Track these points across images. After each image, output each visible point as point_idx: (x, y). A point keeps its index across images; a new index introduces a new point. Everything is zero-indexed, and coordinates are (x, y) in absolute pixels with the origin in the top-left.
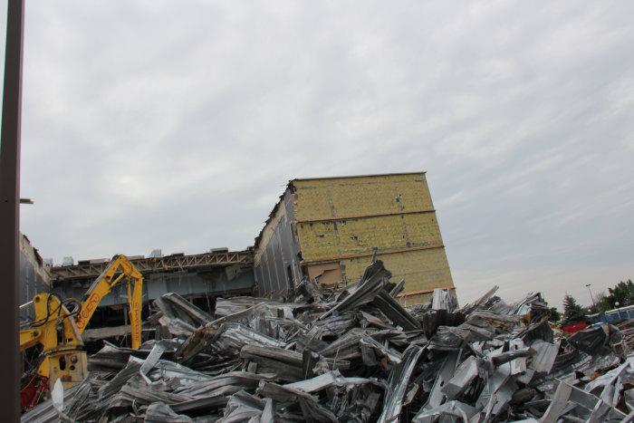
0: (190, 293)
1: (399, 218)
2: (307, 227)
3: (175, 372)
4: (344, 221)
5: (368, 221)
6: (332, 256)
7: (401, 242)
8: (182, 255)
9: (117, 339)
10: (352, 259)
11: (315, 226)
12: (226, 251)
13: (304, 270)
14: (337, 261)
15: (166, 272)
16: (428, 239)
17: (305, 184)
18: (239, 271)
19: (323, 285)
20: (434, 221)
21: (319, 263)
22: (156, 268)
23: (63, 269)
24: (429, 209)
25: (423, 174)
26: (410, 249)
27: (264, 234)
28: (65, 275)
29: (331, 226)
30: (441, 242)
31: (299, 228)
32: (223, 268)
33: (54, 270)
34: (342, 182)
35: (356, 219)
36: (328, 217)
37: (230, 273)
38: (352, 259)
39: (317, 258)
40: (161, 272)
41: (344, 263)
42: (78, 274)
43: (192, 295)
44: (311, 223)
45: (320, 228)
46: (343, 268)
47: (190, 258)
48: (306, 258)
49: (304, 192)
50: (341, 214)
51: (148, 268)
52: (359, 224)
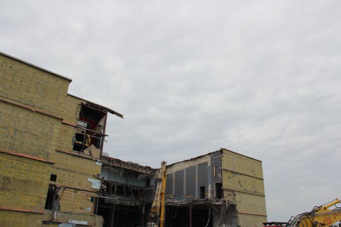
4: (237, 173)
6: (232, 188)
7: (253, 190)
14: (233, 191)
15: (115, 168)
17: (227, 152)
18: (144, 178)
21: (228, 190)
22: (111, 164)
25: (261, 162)
30: (264, 193)
32: (139, 173)
34: (238, 155)
35: (241, 174)
39: (227, 188)
44: (227, 171)
45: (229, 173)
46: (235, 195)
47: (124, 163)
48: (224, 187)
50: (236, 170)
51: (107, 163)
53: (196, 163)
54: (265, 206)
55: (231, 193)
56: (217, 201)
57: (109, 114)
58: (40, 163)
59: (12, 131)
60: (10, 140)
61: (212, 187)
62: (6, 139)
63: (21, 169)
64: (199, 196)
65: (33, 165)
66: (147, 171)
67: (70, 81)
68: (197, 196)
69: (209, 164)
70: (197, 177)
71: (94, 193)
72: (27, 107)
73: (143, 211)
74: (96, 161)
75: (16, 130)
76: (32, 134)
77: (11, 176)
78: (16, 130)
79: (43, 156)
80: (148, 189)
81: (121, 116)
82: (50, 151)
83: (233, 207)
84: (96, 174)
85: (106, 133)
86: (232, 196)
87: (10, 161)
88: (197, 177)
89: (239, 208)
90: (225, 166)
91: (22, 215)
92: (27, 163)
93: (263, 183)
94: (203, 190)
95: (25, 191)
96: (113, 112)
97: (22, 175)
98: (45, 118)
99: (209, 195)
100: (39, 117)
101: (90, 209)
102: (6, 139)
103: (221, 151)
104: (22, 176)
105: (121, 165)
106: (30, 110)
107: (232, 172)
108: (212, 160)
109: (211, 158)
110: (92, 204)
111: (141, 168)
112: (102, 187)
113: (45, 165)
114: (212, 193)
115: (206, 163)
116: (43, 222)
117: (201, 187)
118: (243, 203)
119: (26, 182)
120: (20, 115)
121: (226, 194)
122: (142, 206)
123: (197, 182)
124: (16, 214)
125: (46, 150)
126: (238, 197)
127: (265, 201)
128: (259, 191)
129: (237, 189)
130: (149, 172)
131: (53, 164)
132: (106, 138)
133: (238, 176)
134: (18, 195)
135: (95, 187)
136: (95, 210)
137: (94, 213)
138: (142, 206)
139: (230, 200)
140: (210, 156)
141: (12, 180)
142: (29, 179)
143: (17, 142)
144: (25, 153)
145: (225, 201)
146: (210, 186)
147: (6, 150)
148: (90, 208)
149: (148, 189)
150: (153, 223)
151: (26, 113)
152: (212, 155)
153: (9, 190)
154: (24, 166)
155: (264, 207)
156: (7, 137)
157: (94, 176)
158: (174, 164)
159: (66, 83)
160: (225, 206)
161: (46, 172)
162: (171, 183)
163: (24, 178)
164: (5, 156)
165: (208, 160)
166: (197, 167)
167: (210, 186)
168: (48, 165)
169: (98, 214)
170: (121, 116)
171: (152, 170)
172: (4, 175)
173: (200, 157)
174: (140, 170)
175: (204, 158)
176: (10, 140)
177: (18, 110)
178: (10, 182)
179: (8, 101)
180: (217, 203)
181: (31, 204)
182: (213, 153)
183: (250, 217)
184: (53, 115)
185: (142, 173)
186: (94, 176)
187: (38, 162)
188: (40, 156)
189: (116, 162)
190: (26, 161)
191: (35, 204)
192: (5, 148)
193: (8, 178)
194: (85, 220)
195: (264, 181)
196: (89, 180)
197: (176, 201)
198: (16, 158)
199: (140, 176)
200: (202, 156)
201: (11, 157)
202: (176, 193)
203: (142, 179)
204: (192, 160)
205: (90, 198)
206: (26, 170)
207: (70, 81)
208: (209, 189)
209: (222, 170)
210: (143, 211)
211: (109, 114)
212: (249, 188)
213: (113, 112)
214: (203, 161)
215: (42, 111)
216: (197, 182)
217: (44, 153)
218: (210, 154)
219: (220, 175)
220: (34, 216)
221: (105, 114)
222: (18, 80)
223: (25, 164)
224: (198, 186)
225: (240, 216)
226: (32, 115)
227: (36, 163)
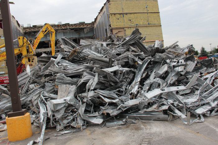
0: (72, 37)
1: (146, 14)
2: (113, 15)
3: (66, 63)
4: (126, 14)
5: (135, 14)
6: (121, 27)
7: (146, 23)
8: (69, 24)
9: (47, 52)
10: (128, 28)
11: (116, 15)
12: (85, 23)
13: (111, 30)
14: (123, 28)
15: (64, 30)
16: (156, 22)
19: (118, 36)
20: (159, 16)
21: (117, 29)
22: (59, 28)
23: (27, 28)
24: (158, 11)
26: (149, 25)
27: (98, 17)
28: (28, 30)
29: (122, 15)
31: (110, 16)
32: (83, 29)
33: (24, 28)
35: (131, 13)
36: (121, 12)
37: (85, 30)
38: (128, 28)
39: (116, 27)
40: (61, 30)
41: (126, 29)
42: (33, 30)
43: (72, 38)
44: (115, 14)
45: (118, 16)
46: (125, 30)
47: (72, 25)
48: (112, 26)
49: (113, 3)
50: (125, 11)
52: (132, 15)
105: (67, 27)
162: (101, 31)
189: (63, 26)
194: (3, 71)
195: (161, 14)
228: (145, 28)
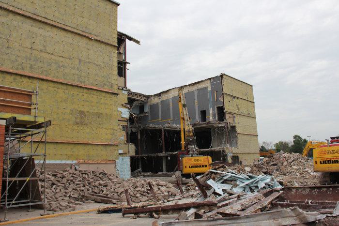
4: (234, 97)
6: (232, 111)
21: (229, 113)
27: (172, 91)
35: (237, 98)
39: (228, 111)
41: (235, 115)
46: (234, 117)
50: (234, 95)
53: (195, 88)
54: (256, 127)
55: (231, 116)
56: (219, 124)
57: (127, 41)
58: (107, 95)
59: (77, 62)
60: (77, 72)
61: (213, 110)
62: (73, 71)
63: (92, 102)
64: (200, 120)
65: (102, 97)
66: (141, 98)
67: (118, 5)
68: (198, 119)
69: (209, 89)
70: (196, 101)
71: (124, 122)
72: (84, 34)
73: (139, 137)
74: (122, 89)
75: (80, 61)
76: (94, 64)
77: (85, 109)
78: (80, 61)
79: (108, 86)
80: (142, 115)
81: (138, 42)
82: (113, 82)
83: (233, 128)
84: (123, 103)
85: (127, 61)
86: (232, 119)
87: (81, 94)
88: (196, 101)
89: (238, 130)
90: (225, 91)
91: (102, 148)
92: (96, 95)
93: (254, 106)
94: (204, 114)
95: (100, 124)
96: (131, 39)
97: (94, 108)
98: (103, 46)
99: (211, 118)
100: (97, 44)
101: (123, 138)
102: (73, 71)
103: (222, 76)
104: (94, 110)
106: (89, 38)
107: (231, 96)
108: (212, 85)
109: (211, 83)
110: (124, 133)
111: (136, 95)
112: (131, 115)
113: (111, 96)
114: (214, 116)
115: (206, 88)
116: (262, 147)
117: (201, 111)
118: (240, 124)
119: (99, 115)
120: (80, 44)
121: (227, 116)
122: (137, 132)
123: (197, 106)
124: (97, 147)
125: (110, 80)
126: (237, 119)
127: (256, 122)
128: (251, 113)
129: (235, 112)
130: (143, 99)
131: (117, 94)
132: (128, 66)
133: (236, 100)
134: (95, 129)
135: (125, 117)
136: (127, 138)
137: (127, 141)
138: (137, 132)
139: (231, 122)
140: (209, 81)
141: (87, 114)
142: (101, 112)
143: (83, 74)
144: (92, 84)
145: (227, 124)
146: (211, 110)
147: (75, 83)
148: (122, 137)
149: (142, 115)
150: (193, 146)
151: (85, 41)
152: (212, 80)
153: (86, 124)
154: (94, 98)
155: (255, 128)
156: (74, 68)
157: (122, 105)
158: (170, 90)
159: (114, 7)
160: (228, 128)
161: (113, 103)
163: (96, 111)
164: (76, 89)
165: (208, 85)
166: (196, 93)
167: (211, 110)
168: (113, 96)
169: (131, 142)
170: (138, 42)
171: (146, 97)
172: (79, 110)
173: (198, 83)
174: (135, 97)
175: (203, 82)
176: (77, 72)
177: (77, 38)
178: (85, 116)
179: (67, 28)
180: (220, 126)
181: (107, 137)
182: (213, 78)
183: (245, 136)
184: (109, 42)
185: (137, 100)
186: (122, 105)
187: (105, 93)
188: (106, 87)
190: (95, 93)
191: (110, 136)
192: (74, 80)
193: (82, 113)
196: (120, 109)
197: (175, 125)
198: (85, 91)
199: (135, 103)
200: (202, 81)
201: (81, 90)
202: (174, 118)
203: (136, 106)
204: (190, 85)
205: (121, 127)
206: (97, 103)
207: (118, 5)
208: (211, 112)
209: (223, 94)
210: (139, 137)
211: (127, 41)
212: (245, 111)
213: (131, 39)
214: (202, 86)
215: (98, 39)
216: (197, 106)
217: (108, 84)
218: (210, 79)
219: (222, 99)
220: (111, 148)
221: (124, 41)
222: (71, 4)
223: (94, 96)
224: (198, 108)
225: (239, 136)
226: (91, 43)
227: (104, 94)
228: (247, 118)
